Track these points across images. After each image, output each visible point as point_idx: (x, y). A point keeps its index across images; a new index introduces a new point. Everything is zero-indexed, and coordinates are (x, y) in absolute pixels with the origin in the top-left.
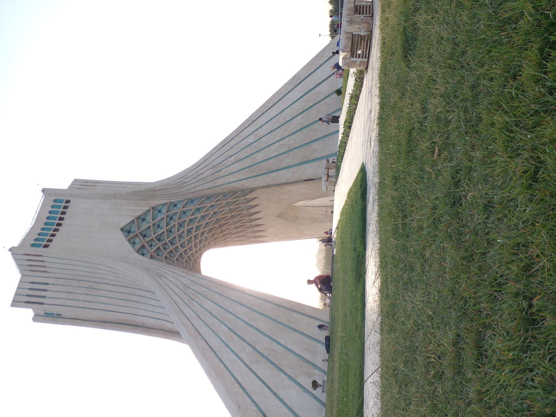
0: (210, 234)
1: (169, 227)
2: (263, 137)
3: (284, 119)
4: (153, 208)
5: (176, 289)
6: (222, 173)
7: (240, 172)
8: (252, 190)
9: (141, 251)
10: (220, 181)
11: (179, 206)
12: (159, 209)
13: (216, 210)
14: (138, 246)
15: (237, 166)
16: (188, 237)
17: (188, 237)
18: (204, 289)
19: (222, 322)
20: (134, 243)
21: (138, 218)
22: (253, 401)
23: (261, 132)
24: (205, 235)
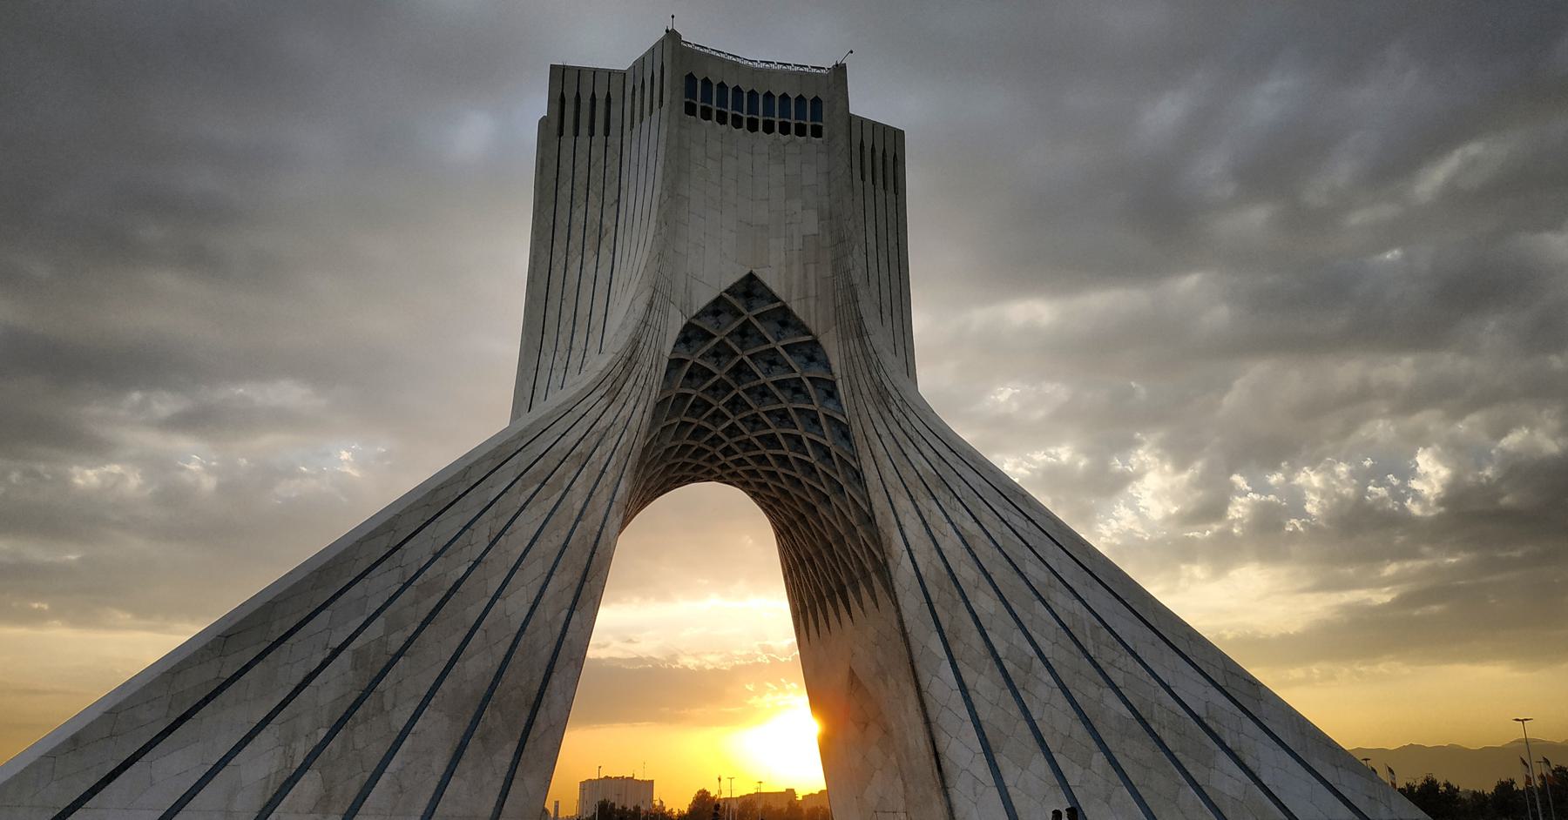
0: (777, 495)
1: (773, 388)
2: (1048, 607)
3: (1111, 664)
4: (815, 342)
6: (925, 503)
7: (935, 554)
9: (691, 334)
10: (903, 503)
11: (831, 405)
13: (833, 499)
14: (707, 324)
15: (950, 543)
18: (579, 505)
19: (477, 563)
20: (716, 313)
21: (785, 310)
22: (247, 668)
23: (1061, 600)
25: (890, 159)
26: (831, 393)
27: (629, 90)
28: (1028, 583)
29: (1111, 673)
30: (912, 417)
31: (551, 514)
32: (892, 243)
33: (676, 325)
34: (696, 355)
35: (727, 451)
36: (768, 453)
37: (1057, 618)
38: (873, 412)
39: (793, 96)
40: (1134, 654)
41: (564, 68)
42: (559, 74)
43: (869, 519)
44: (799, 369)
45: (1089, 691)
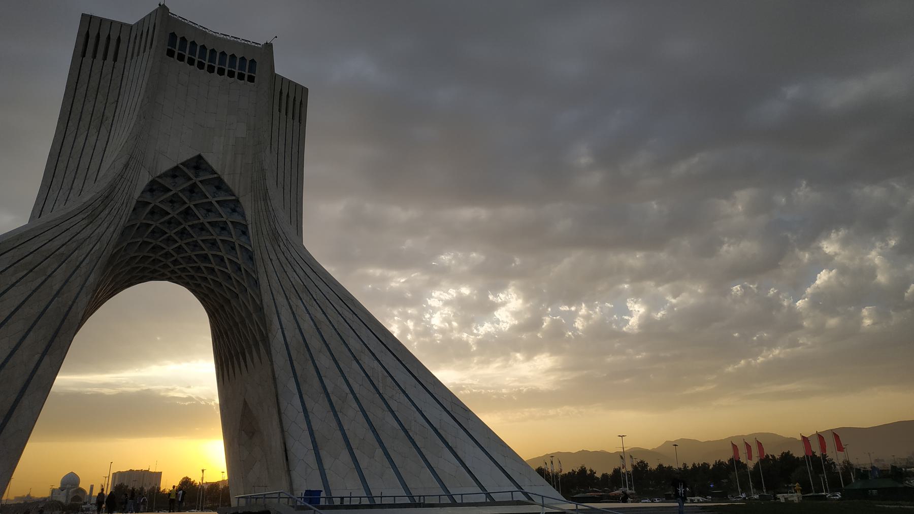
1: (208, 225)
4: (237, 201)
5: (57, 243)
6: (295, 301)
7: (297, 331)
8: (269, 353)
10: (281, 300)
11: (243, 239)
12: (238, 209)
13: (240, 296)
14: (167, 182)
15: (307, 325)
16: (195, 258)
17: (195, 258)
18: (56, 287)
20: (174, 176)
21: (220, 179)
23: (367, 360)
24: (203, 284)
25: (298, 103)
26: (245, 233)
27: (133, 35)
28: (350, 350)
29: (390, 402)
30: (292, 250)
31: (34, 291)
32: (295, 150)
33: (144, 180)
34: (157, 201)
35: (175, 262)
36: (202, 265)
37: (364, 371)
38: (268, 244)
39: (239, 56)
40: (404, 392)
41: (91, 17)
42: (88, 20)
43: (260, 309)
44: (226, 216)
45: (378, 414)
